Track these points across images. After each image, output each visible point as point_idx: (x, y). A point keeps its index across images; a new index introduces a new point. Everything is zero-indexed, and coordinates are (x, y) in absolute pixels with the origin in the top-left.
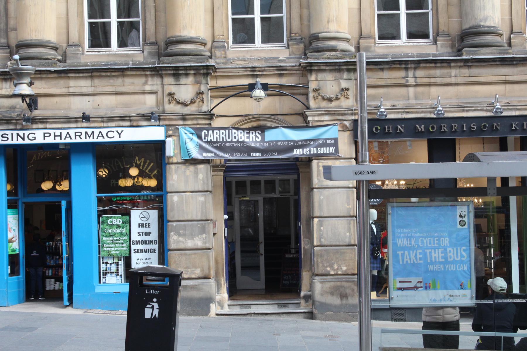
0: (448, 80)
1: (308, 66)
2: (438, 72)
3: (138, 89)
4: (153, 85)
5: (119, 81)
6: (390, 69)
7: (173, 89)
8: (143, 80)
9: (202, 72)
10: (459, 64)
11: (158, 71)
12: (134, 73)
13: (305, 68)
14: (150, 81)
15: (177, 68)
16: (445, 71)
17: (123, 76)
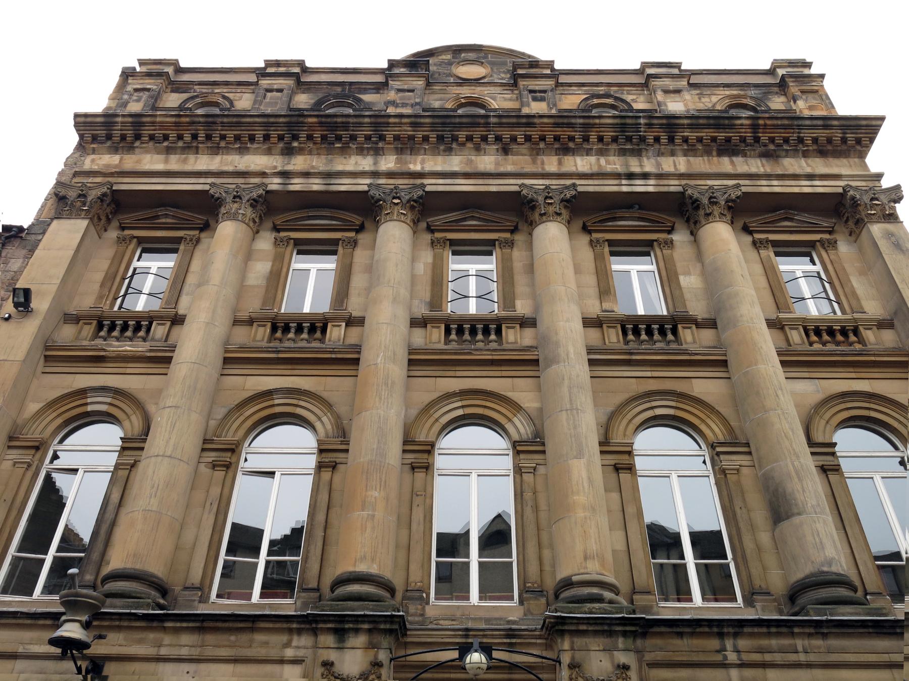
0: (792, 657)
1: (557, 624)
2: (774, 642)
3: (274, 653)
4: (298, 647)
5: (244, 638)
6: (692, 635)
7: (332, 656)
8: (284, 638)
9: (382, 626)
10: (807, 630)
11: (310, 623)
12: (271, 625)
13: (554, 625)
14: (296, 641)
15: (342, 619)
16: (786, 642)
17: (253, 630)
